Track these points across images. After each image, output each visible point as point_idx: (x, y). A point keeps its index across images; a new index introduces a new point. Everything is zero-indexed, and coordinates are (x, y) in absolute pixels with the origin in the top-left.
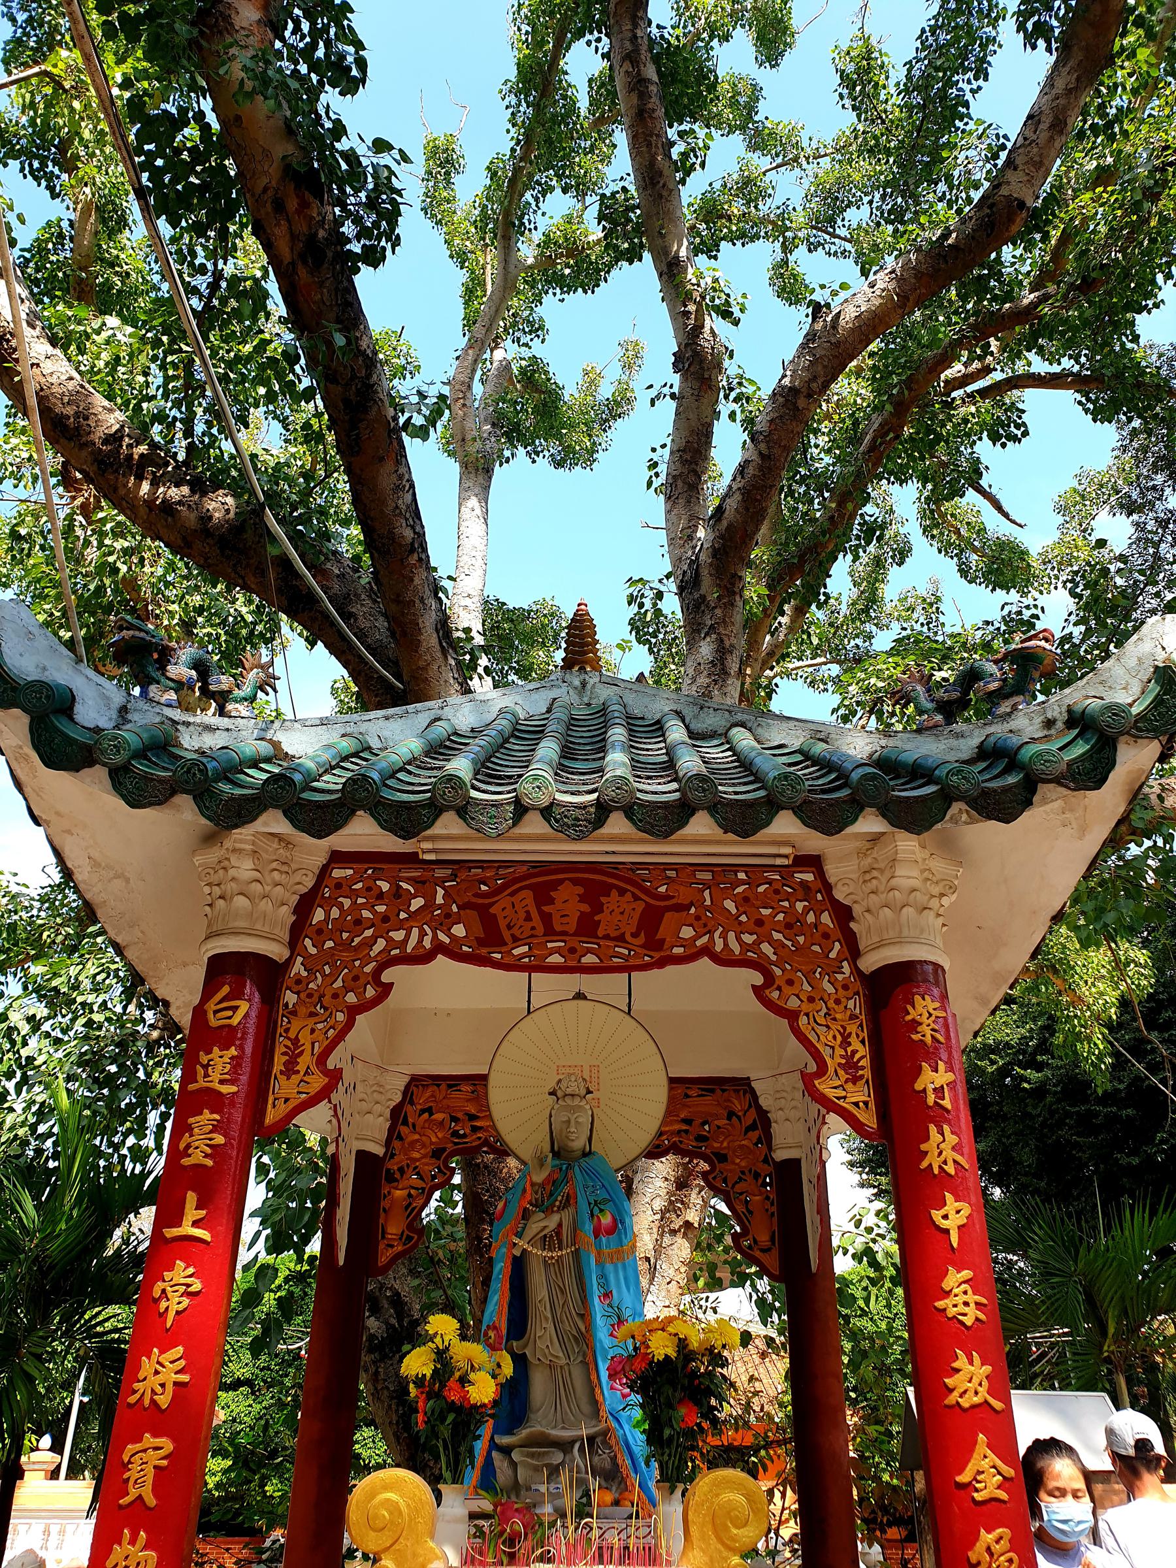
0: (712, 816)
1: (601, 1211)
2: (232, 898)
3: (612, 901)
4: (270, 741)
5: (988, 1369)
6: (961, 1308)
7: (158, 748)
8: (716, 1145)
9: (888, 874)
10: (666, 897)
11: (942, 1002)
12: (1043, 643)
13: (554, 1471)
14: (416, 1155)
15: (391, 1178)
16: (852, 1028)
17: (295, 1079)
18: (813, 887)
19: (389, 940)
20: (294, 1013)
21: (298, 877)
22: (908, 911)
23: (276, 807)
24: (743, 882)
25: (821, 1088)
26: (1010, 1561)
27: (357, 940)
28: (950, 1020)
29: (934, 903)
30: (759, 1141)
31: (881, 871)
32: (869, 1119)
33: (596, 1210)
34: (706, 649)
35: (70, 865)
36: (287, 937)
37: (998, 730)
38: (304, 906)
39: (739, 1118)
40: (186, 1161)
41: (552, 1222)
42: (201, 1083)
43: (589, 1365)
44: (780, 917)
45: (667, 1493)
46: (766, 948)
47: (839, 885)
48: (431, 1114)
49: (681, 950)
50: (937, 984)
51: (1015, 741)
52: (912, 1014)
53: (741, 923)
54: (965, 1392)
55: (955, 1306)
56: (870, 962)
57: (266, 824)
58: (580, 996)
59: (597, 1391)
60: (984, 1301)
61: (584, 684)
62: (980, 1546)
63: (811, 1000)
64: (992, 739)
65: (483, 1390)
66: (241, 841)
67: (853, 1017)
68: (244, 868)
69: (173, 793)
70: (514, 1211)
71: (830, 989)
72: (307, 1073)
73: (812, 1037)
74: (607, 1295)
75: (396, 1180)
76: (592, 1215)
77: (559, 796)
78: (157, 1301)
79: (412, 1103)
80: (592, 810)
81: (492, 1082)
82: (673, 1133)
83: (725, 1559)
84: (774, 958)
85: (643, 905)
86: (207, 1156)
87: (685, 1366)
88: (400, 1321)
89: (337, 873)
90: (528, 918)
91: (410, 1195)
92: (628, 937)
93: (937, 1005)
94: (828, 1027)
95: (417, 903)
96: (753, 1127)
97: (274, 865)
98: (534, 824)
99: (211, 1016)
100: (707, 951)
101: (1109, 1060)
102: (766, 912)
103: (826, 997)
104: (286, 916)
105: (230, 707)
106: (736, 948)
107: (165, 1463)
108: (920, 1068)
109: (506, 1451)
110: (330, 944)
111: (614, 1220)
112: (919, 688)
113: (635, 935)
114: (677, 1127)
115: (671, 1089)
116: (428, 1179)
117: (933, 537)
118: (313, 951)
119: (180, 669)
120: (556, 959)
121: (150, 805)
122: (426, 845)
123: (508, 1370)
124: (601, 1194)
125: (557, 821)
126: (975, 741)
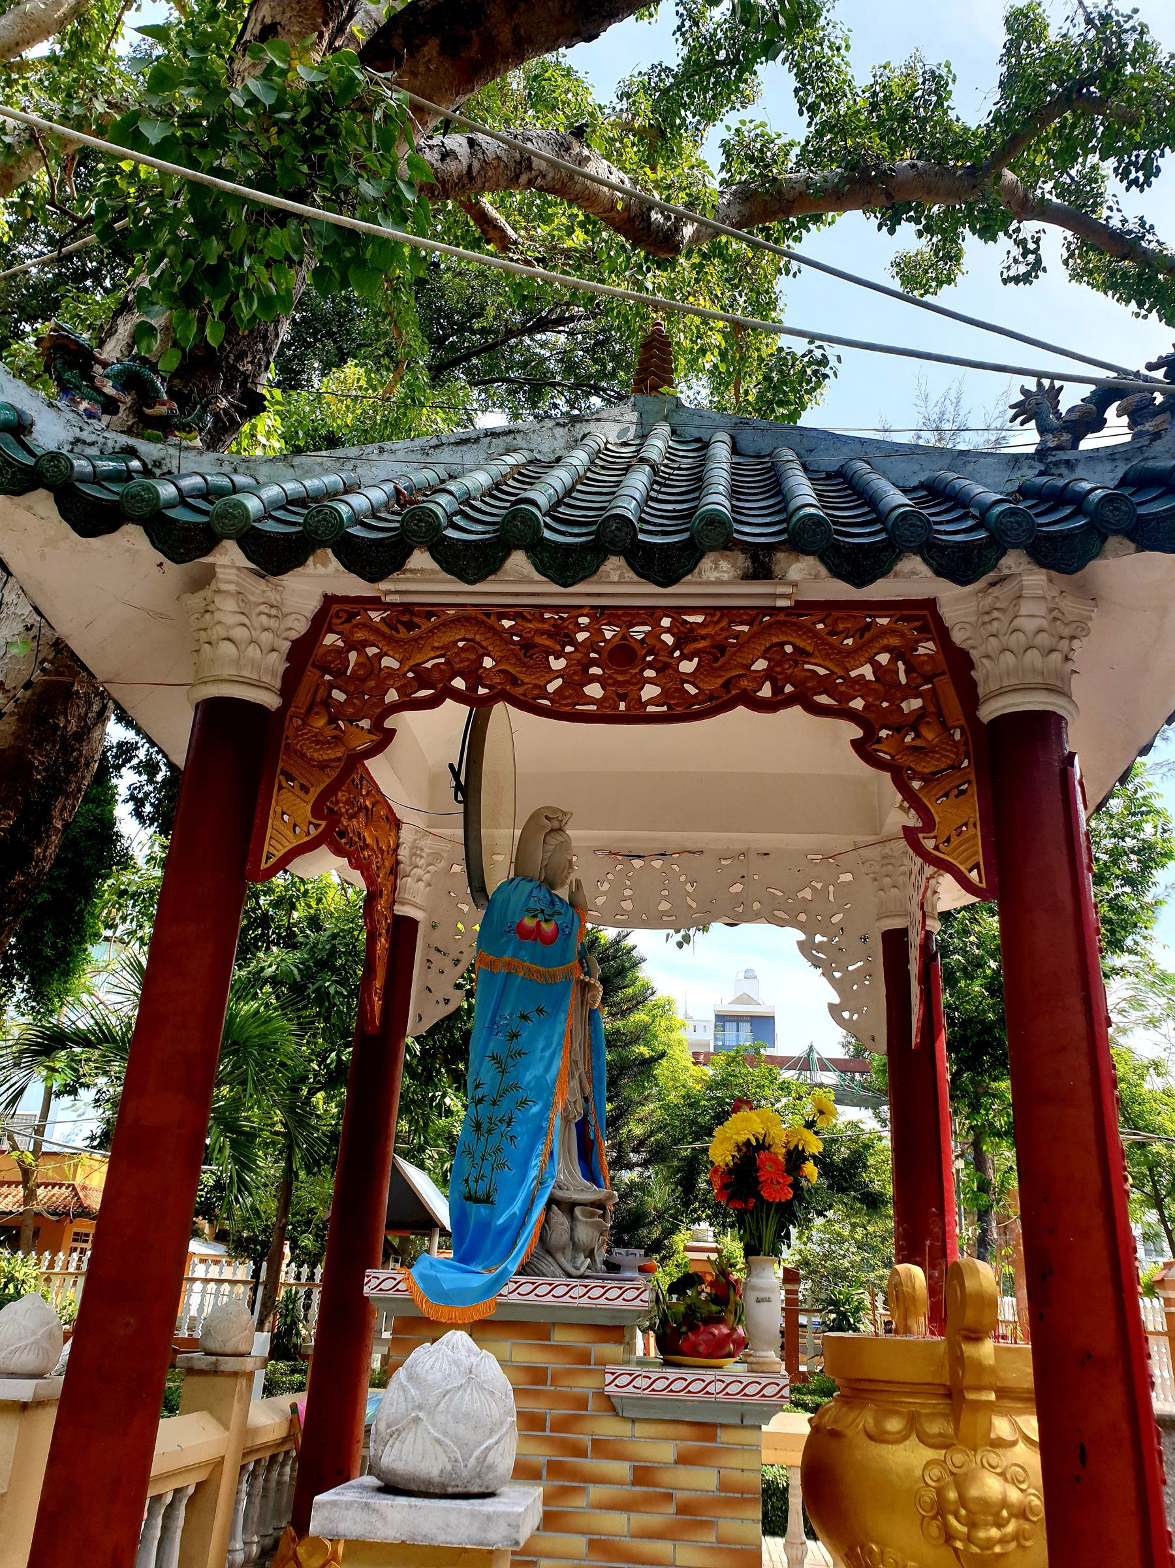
36: (278, 684)
97: (262, 608)
104: (277, 663)
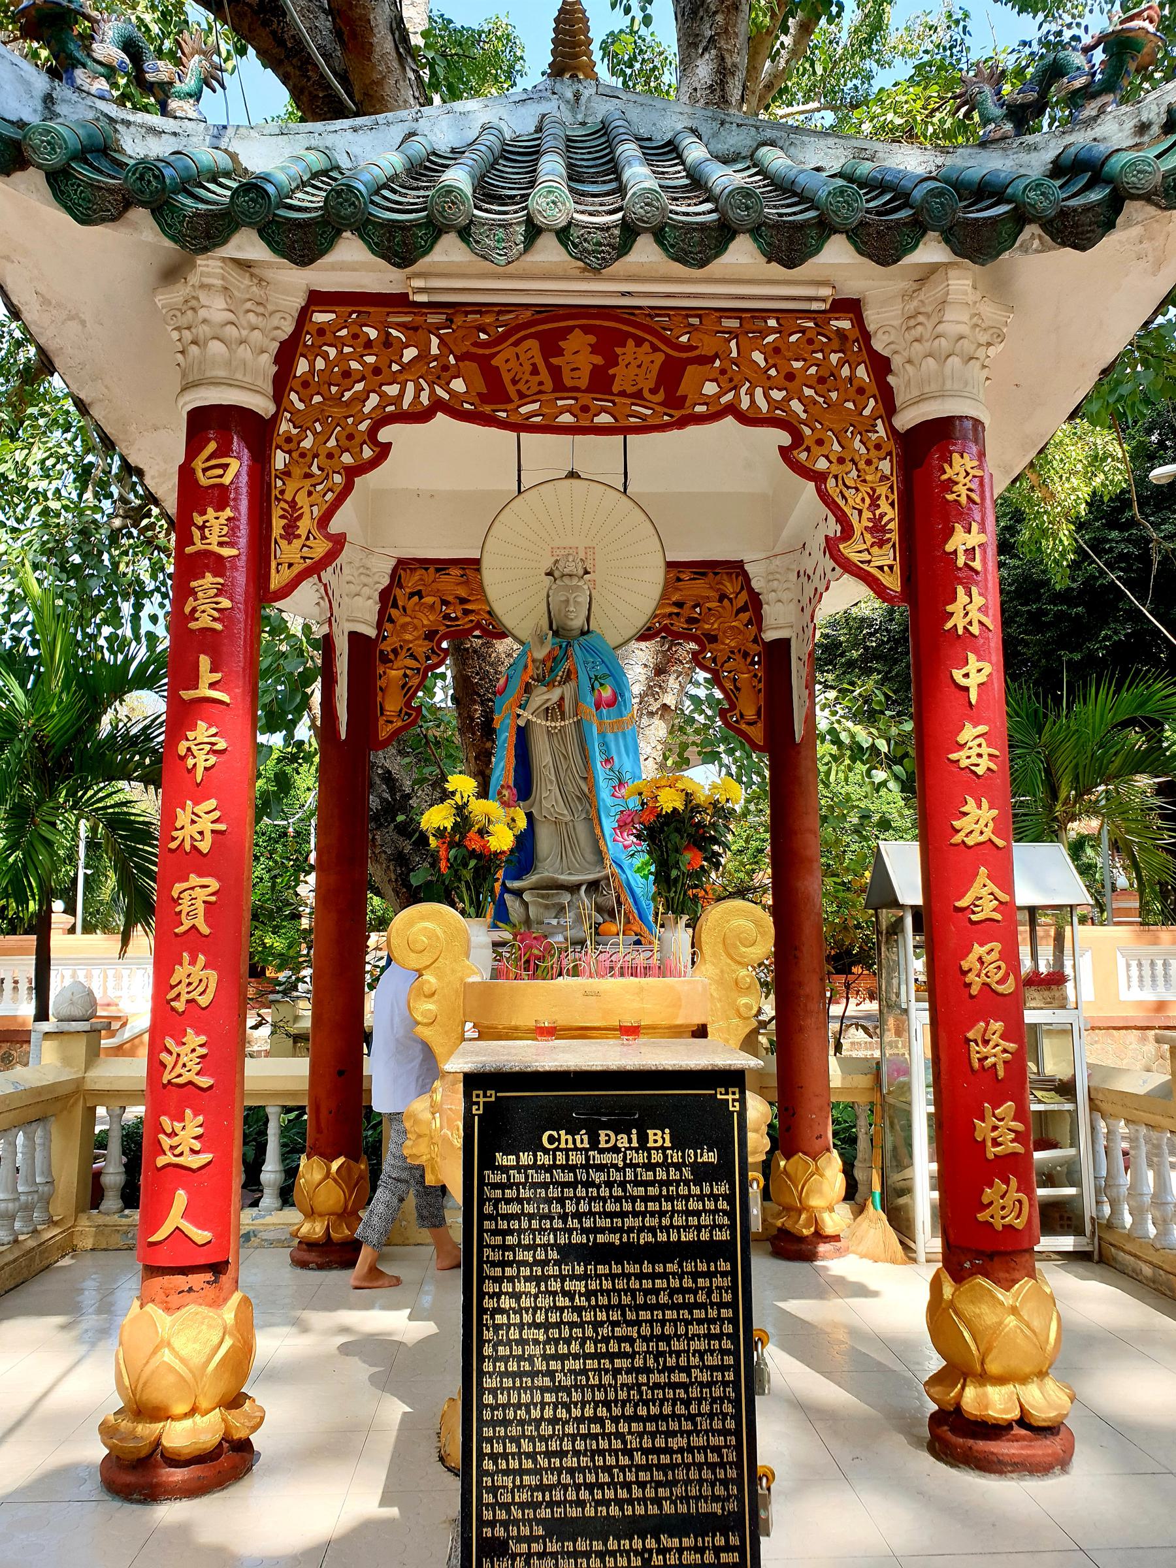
0: (756, 240)
2: (206, 344)
3: (628, 352)
4: (226, 151)
5: (995, 812)
6: (974, 760)
7: (98, 151)
10: (688, 348)
13: (561, 910)
14: (408, 637)
15: (385, 660)
16: (882, 490)
17: (297, 543)
18: (852, 337)
19: (382, 395)
20: (287, 473)
21: (275, 321)
22: (955, 361)
23: (250, 225)
24: (773, 331)
25: (845, 552)
26: (999, 968)
27: (347, 395)
28: (987, 480)
29: (981, 353)
30: (750, 622)
31: (928, 316)
32: (893, 582)
33: (597, 684)
34: (704, 70)
35: (15, 302)
37: (1080, 139)
38: (286, 354)
39: (730, 600)
40: (193, 625)
42: (199, 546)
43: (593, 820)
46: (796, 405)
47: (880, 332)
48: (421, 597)
49: (704, 408)
50: (976, 442)
51: (1103, 148)
52: (949, 473)
53: (769, 377)
56: (905, 420)
57: (239, 248)
58: (573, 475)
59: (601, 843)
61: (577, 96)
62: (972, 957)
63: (841, 461)
64: (1073, 150)
65: (502, 840)
66: (209, 275)
68: (215, 308)
69: (127, 205)
70: (516, 686)
71: (863, 450)
72: (308, 538)
73: (841, 503)
74: (609, 760)
75: (391, 661)
77: (577, 216)
78: (183, 758)
79: (400, 586)
80: (617, 232)
81: (485, 565)
82: (664, 616)
84: (804, 416)
86: (215, 619)
87: (692, 818)
88: (393, 795)
89: (320, 318)
90: (535, 371)
91: (405, 675)
92: (646, 394)
93: (975, 463)
94: (857, 489)
95: (410, 354)
96: (743, 609)
97: (249, 305)
98: (549, 252)
99: (200, 474)
100: (732, 409)
102: (797, 365)
103: (857, 458)
104: (266, 365)
105: (173, 104)
106: (763, 405)
107: (213, 899)
108: (953, 529)
109: (518, 893)
110: (317, 399)
111: (614, 694)
112: (987, 89)
113: (653, 391)
114: (668, 610)
115: (667, 572)
116: (422, 658)
118: (301, 406)
119: (107, 49)
120: (566, 418)
121: (103, 220)
122: (418, 283)
123: (522, 824)
124: (601, 669)
125: (575, 246)
126: (1049, 155)
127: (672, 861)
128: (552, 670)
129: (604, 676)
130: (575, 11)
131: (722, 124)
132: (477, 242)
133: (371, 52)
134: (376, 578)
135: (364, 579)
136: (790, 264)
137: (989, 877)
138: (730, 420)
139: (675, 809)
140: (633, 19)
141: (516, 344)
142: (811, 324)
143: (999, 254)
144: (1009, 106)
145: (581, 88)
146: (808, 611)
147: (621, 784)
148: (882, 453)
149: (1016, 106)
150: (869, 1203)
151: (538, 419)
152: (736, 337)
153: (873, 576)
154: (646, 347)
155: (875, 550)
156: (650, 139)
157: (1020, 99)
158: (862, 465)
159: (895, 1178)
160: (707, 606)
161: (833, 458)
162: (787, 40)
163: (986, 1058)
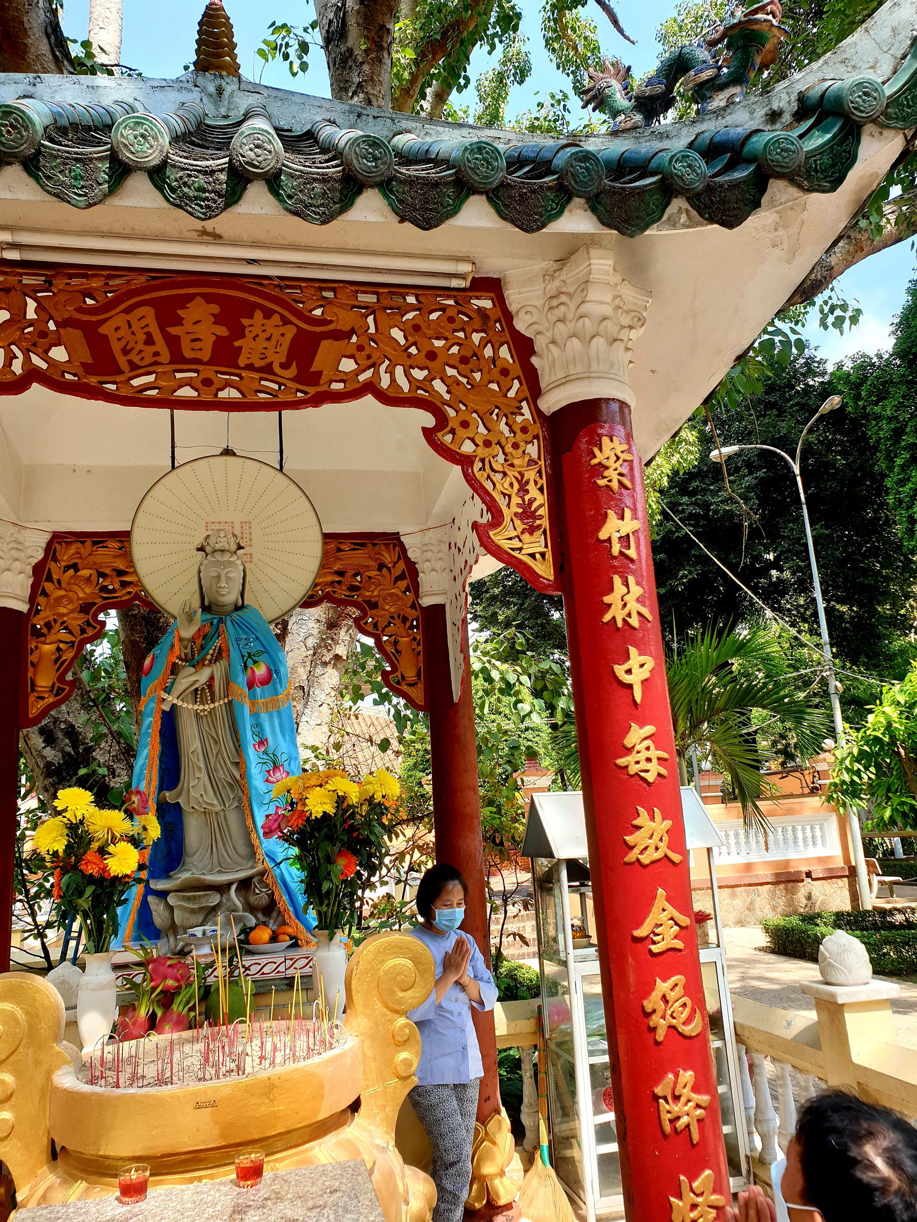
0: (386, 196)
1: (255, 662)
6: (644, 765)
8: (368, 594)
9: (578, 299)
11: (628, 443)
12: (770, 17)
14: (63, 610)
15: (37, 634)
16: (531, 475)
18: (493, 317)
22: (599, 342)
24: (412, 308)
25: (496, 539)
26: (684, 1005)
29: (623, 335)
31: (570, 296)
33: (250, 663)
37: (710, 127)
39: (389, 569)
41: (203, 676)
43: (245, 808)
44: (455, 349)
45: (324, 940)
46: (438, 385)
48: (77, 570)
52: (600, 457)
53: (410, 356)
54: (646, 848)
55: (637, 762)
56: (551, 403)
58: (228, 452)
60: (665, 755)
62: (656, 995)
63: (487, 444)
65: (124, 861)
67: (532, 462)
73: (488, 485)
74: (262, 743)
75: (44, 635)
76: (246, 667)
79: (55, 560)
80: (223, 177)
81: (136, 538)
83: (391, 1021)
84: (447, 397)
85: (295, 330)
88: (75, 748)
90: (149, 341)
91: (59, 649)
92: (277, 368)
93: (625, 447)
94: (505, 474)
96: (401, 577)
98: (140, 195)
100: (371, 388)
101: (658, 517)
102: (439, 343)
103: (503, 442)
108: (606, 516)
111: (269, 671)
114: (330, 578)
115: (325, 544)
117: (554, 50)
120: (186, 392)
123: (155, 831)
124: (254, 646)
125: (173, 190)
127: (323, 872)
128: (202, 648)
129: (259, 653)
130: (219, 17)
131: (359, 116)
132: (49, 178)
133: (25, 52)
134: (29, 552)
135: (15, 554)
136: (427, 224)
137: (668, 899)
138: (369, 398)
139: (325, 813)
140: (291, 63)
141: (127, 311)
142: (451, 302)
143: (647, 227)
144: (637, 98)
145: (224, 84)
146: (460, 581)
147: (276, 768)
148: (529, 437)
149: (645, 98)
150: (537, 1156)
151: (154, 392)
152: (373, 312)
153: (525, 564)
154: (276, 319)
155: (526, 537)
156: (290, 131)
157: (648, 91)
158: (509, 448)
159: (562, 1129)
160: (363, 574)
161: (479, 441)
162: (426, 105)
163: (678, 1118)
